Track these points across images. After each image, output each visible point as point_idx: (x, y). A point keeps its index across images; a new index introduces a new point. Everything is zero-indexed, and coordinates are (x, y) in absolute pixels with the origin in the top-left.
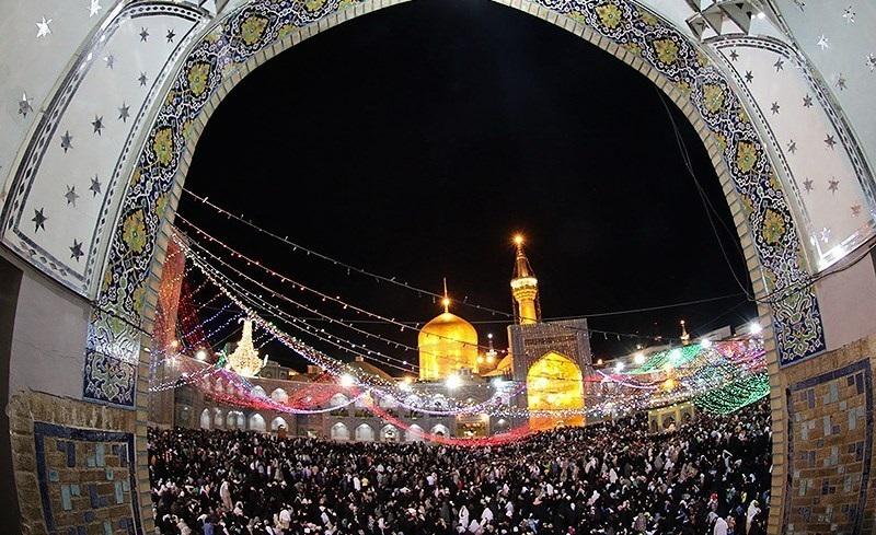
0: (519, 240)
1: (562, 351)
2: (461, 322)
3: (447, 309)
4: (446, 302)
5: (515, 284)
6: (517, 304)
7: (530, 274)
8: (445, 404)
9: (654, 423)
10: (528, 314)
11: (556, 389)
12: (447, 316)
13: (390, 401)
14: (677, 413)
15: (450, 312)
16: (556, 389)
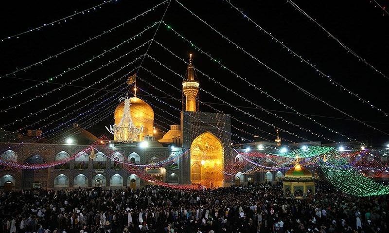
0: (191, 55)
1: (215, 132)
2: (145, 104)
5: (184, 84)
6: (185, 97)
7: (196, 80)
8: (138, 159)
9: (288, 190)
10: (191, 107)
11: (207, 157)
13: (100, 157)
14: (304, 187)
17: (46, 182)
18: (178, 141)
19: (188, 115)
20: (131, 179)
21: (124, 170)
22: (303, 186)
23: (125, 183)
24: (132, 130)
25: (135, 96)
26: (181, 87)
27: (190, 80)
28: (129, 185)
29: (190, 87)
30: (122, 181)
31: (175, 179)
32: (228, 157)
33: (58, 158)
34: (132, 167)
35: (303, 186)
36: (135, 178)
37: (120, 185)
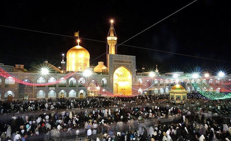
0: (112, 21)
2: (85, 50)
3: (78, 44)
4: (79, 41)
5: (109, 38)
7: (115, 36)
9: (172, 98)
10: (112, 51)
11: (123, 80)
12: (78, 47)
13: (63, 81)
14: (182, 96)
15: (80, 45)
16: (123, 80)
17: (32, 95)
18: (106, 72)
19: (111, 56)
20: (80, 92)
21: (77, 87)
22: (181, 96)
23: (77, 96)
24: (77, 65)
25: (78, 45)
26: (106, 40)
27: (112, 36)
28: (79, 96)
29: (112, 40)
30: (75, 94)
31: (105, 93)
32: (134, 81)
33: (38, 81)
34: (81, 86)
35: (181, 96)
36: (83, 93)
37: (74, 96)
